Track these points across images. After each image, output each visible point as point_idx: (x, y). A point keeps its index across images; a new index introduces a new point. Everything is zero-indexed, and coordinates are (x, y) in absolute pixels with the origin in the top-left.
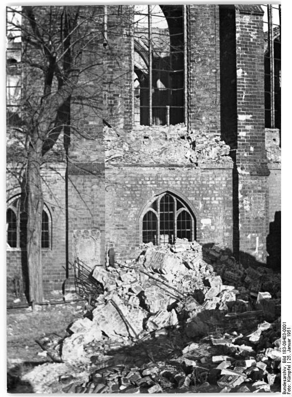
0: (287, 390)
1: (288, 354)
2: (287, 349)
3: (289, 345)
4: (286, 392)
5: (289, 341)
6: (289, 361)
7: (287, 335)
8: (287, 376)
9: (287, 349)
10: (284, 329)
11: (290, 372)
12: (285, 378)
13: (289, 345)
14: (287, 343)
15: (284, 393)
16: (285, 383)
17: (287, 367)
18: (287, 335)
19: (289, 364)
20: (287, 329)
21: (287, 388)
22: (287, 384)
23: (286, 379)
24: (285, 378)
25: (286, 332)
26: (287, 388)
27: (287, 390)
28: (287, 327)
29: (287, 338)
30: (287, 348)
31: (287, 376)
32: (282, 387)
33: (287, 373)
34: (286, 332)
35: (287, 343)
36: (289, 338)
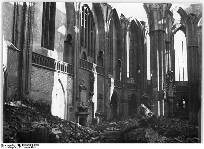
0: (4, 146)
1: (22, 147)
2: (24, 146)
3: (27, 148)
5: (29, 148)
6: (19, 147)
7: (32, 146)
8: (11, 146)
9: (24, 146)
10: (35, 145)
11: (13, 148)
13: (27, 148)
14: (28, 146)
15: (2, 145)
16: (7, 145)
17: (15, 146)
18: (32, 146)
19: (17, 147)
20: (35, 146)
21: (5, 146)
22: (7, 147)
23: (9, 146)
24: (10, 145)
25: (33, 146)
26: (5, 146)
27: (4, 146)
28: (36, 146)
29: (30, 146)
30: (25, 146)
31: (11, 146)
32: (5, 144)
33: (12, 146)
34: (33, 146)
35: (28, 146)
36: (30, 148)
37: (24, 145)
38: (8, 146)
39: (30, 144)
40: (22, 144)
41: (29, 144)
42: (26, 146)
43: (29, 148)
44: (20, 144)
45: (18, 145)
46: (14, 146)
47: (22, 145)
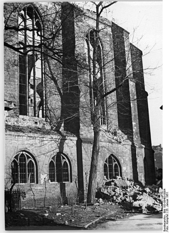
0: (166, 229)
1: (166, 208)
2: (166, 205)
3: (167, 203)
4: (166, 230)
5: (167, 200)
6: (167, 212)
7: (166, 196)
8: (166, 221)
9: (166, 205)
10: (164, 193)
11: (168, 219)
13: (167, 203)
14: (166, 201)
15: (164, 231)
16: (165, 225)
17: (166, 216)
18: (166, 196)
19: (167, 214)
20: (166, 193)
21: (166, 227)
22: (166, 225)
23: (166, 223)
25: (166, 195)
26: (166, 227)
27: (166, 229)
28: (166, 192)
29: (166, 198)
30: (166, 204)
31: (166, 221)
33: (166, 219)
34: (166, 195)
35: (166, 201)
36: (167, 198)
37: (164, 206)
42: (166, 203)
43: (167, 200)
45: (165, 212)
47: (165, 208)
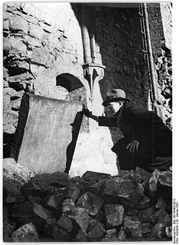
2: (176, 216)
7: (176, 207)
8: (176, 232)
9: (176, 216)
10: (174, 203)
12: (175, 233)
14: (176, 212)
15: (174, 243)
16: (174, 236)
17: (176, 227)
18: (176, 207)
21: (176, 239)
24: (175, 233)
26: (176, 239)
27: (176, 241)
29: (176, 208)
31: (176, 232)
33: (176, 230)
35: (176, 212)
37: (174, 216)
38: (176, 235)
39: (173, 209)
40: (173, 219)
41: (173, 210)
42: (176, 214)
44: (173, 221)
46: (175, 228)
47: (174, 219)
